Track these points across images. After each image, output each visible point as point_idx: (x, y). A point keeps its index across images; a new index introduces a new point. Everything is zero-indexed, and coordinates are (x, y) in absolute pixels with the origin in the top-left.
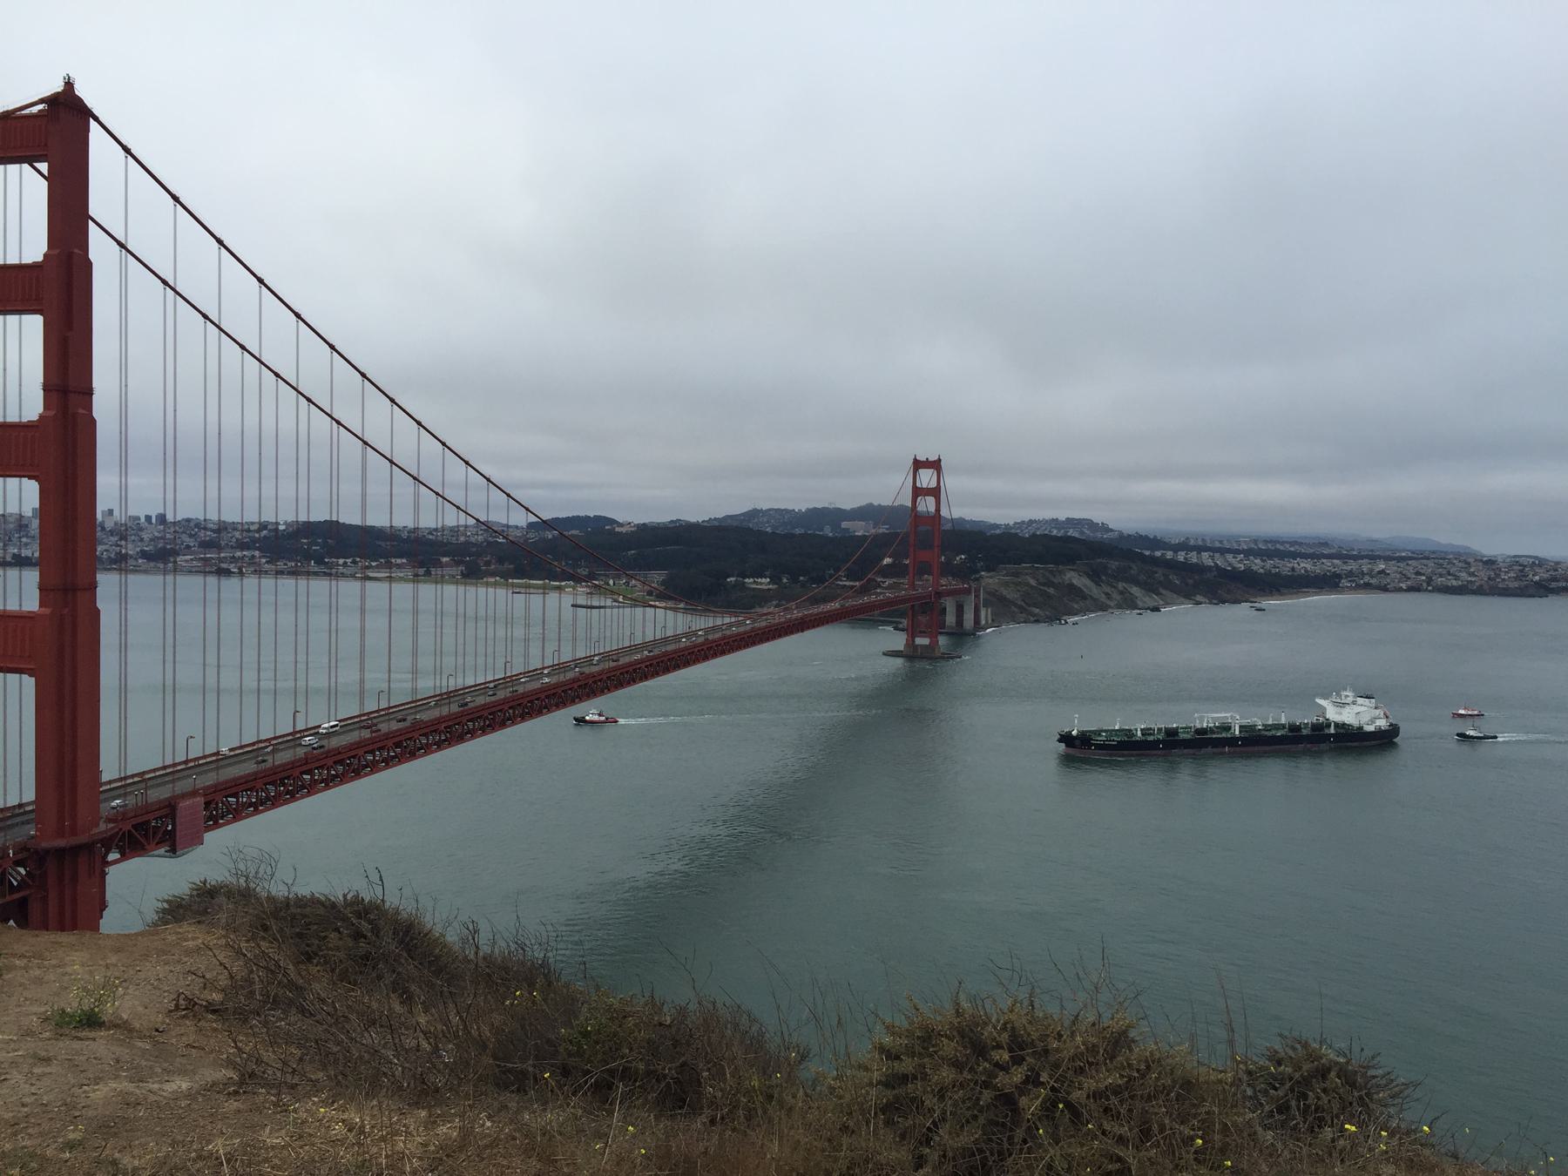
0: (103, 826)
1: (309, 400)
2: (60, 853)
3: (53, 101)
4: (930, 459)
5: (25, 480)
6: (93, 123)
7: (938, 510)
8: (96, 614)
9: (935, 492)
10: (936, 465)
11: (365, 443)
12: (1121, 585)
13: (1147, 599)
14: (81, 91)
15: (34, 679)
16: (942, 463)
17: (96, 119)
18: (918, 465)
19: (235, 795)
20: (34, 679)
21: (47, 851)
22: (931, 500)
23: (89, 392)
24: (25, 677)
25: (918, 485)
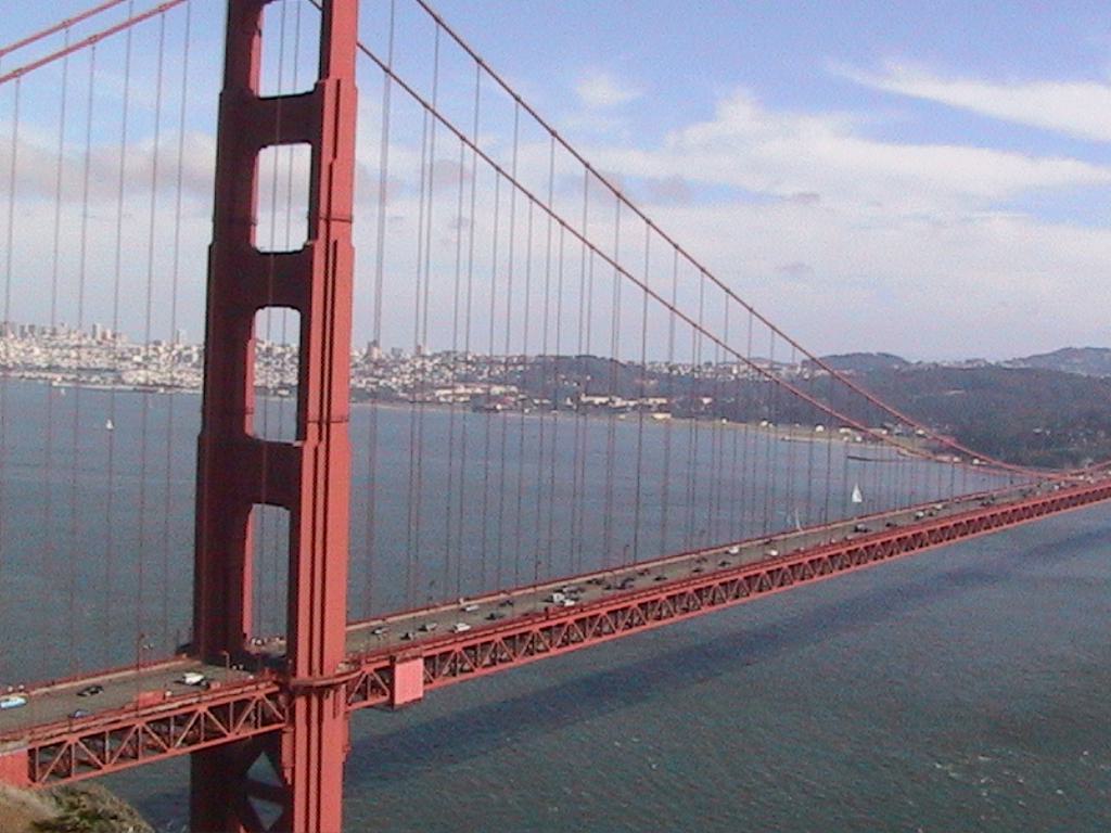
1: (562, 223)
5: (289, 310)
11: (619, 269)
21: (296, 688)
23: (350, 222)
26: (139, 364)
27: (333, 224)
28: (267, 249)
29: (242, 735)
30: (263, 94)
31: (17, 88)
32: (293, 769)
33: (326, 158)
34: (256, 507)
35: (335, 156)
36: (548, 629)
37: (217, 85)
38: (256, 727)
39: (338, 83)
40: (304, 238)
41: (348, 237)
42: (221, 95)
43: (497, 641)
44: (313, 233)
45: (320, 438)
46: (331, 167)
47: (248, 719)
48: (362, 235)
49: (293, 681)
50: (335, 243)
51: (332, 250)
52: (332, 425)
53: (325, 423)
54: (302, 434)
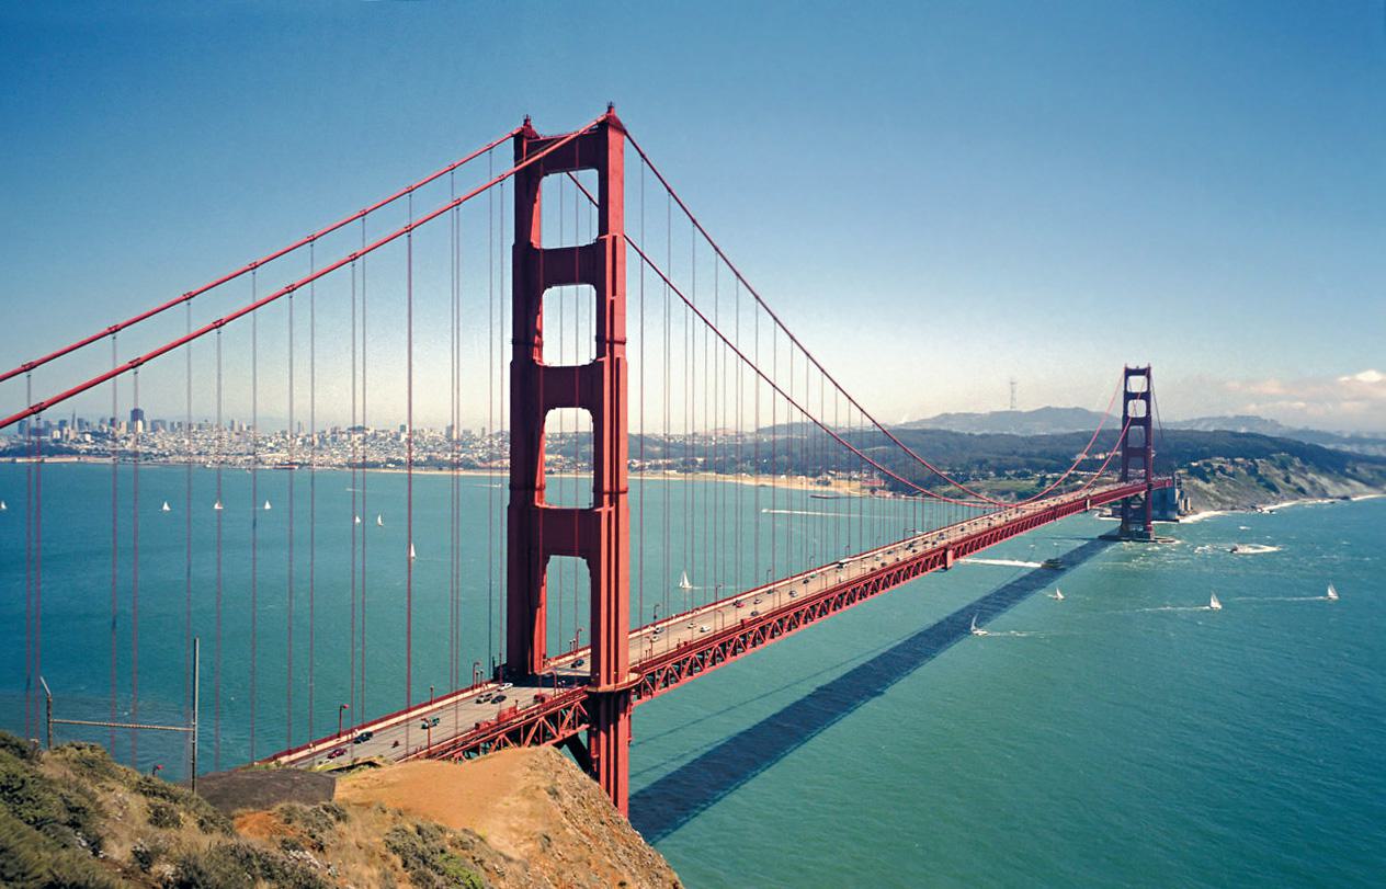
0: (634, 676)
1: (724, 340)
2: (609, 694)
3: (604, 126)
4: (1142, 367)
5: (580, 409)
6: (625, 137)
7: (1148, 411)
8: (628, 510)
9: (1146, 396)
10: (1146, 372)
11: (758, 372)
12: (1311, 476)
13: (1336, 489)
14: (618, 113)
15: (585, 561)
16: (1152, 372)
17: (625, 133)
18: (1129, 373)
19: (702, 653)
20: (585, 561)
21: (602, 694)
22: (1143, 402)
23: (624, 343)
24: (580, 559)
25: (1129, 390)
26: (271, 448)
27: (616, 346)
28: (556, 364)
29: (567, 736)
30: (545, 246)
31: (410, 241)
32: (598, 759)
33: (609, 296)
34: (552, 557)
35: (614, 294)
36: (744, 636)
37: (510, 240)
38: (574, 728)
39: (614, 238)
40: (594, 357)
41: (624, 353)
42: (514, 246)
43: (716, 646)
44: (600, 352)
45: (611, 505)
46: (612, 302)
47: (569, 723)
48: (631, 354)
49: (600, 690)
50: (618, 359)
51: (616, 366)
52: (621, 496)
53: (615, 496)
54: (598, 502)
